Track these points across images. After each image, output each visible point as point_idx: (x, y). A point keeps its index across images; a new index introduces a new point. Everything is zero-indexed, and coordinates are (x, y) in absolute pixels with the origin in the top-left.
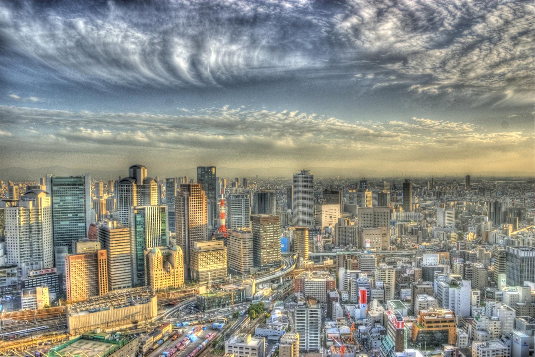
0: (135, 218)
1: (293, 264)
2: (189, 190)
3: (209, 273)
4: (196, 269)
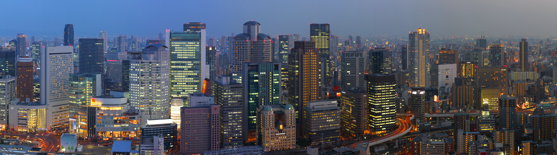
1: (409, 127)
2: (304, 49)
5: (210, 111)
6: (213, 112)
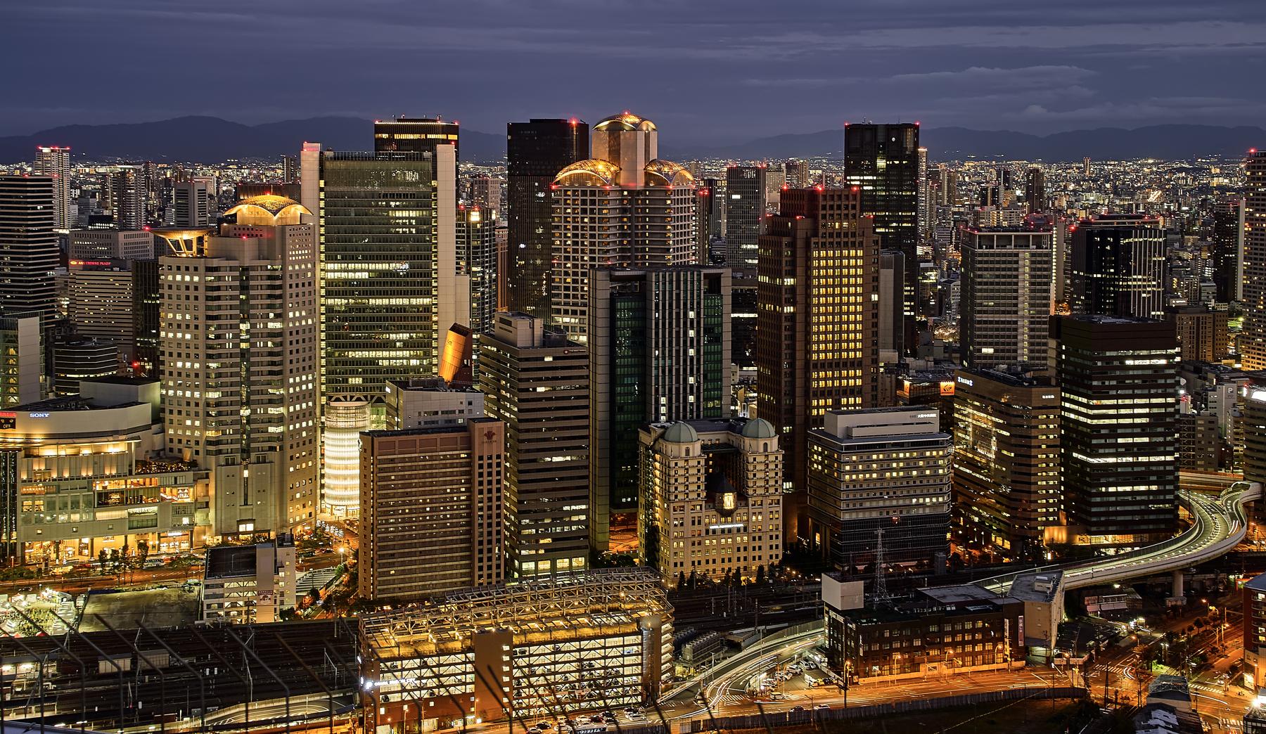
0: (612, 310)
3: (880, 532)
4: (831, 511)
5: (469, 445)
6: (482, 448)
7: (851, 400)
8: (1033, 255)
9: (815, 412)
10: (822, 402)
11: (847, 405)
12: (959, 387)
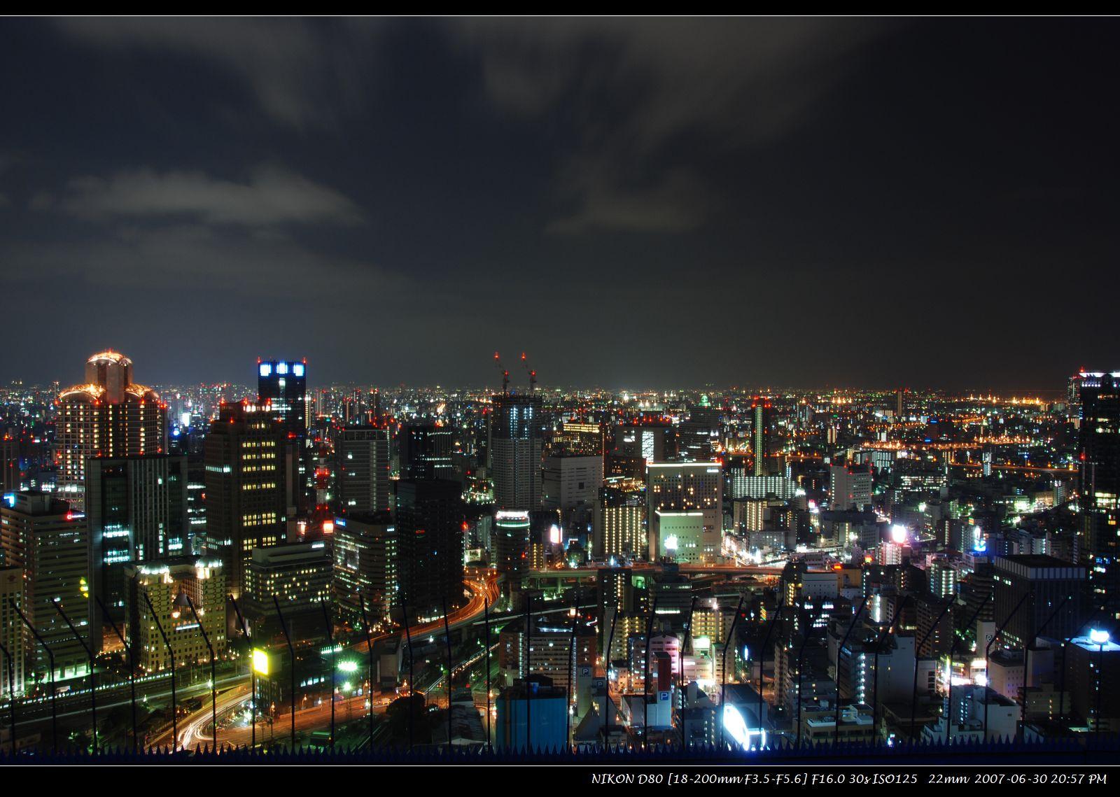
7: (269, 539)
8: (378, 443)
9: (245, 548)
10: (250, 541)
11: (267, 542)
12: (337, 528)
